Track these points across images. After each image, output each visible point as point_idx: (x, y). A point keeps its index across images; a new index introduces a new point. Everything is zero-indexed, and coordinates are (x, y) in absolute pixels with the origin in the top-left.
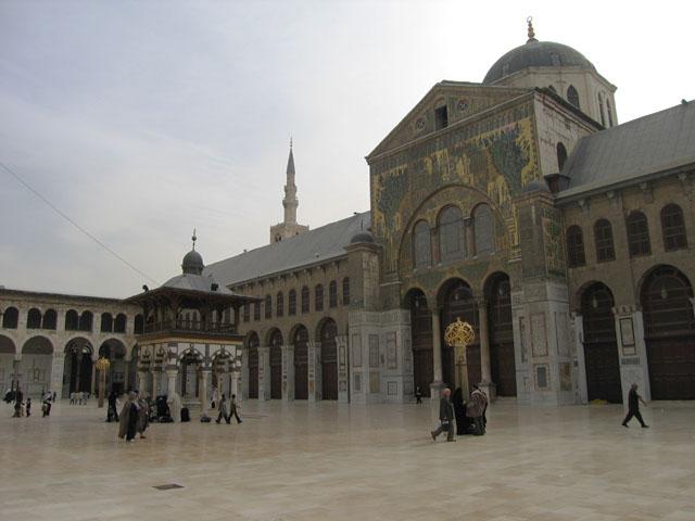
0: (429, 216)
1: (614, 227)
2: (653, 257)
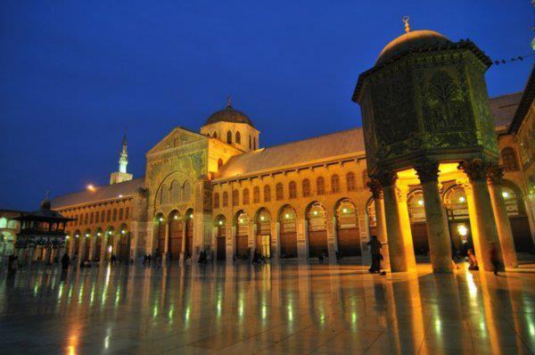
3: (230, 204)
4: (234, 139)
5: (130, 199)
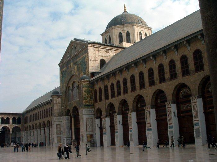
0: (70, 85)
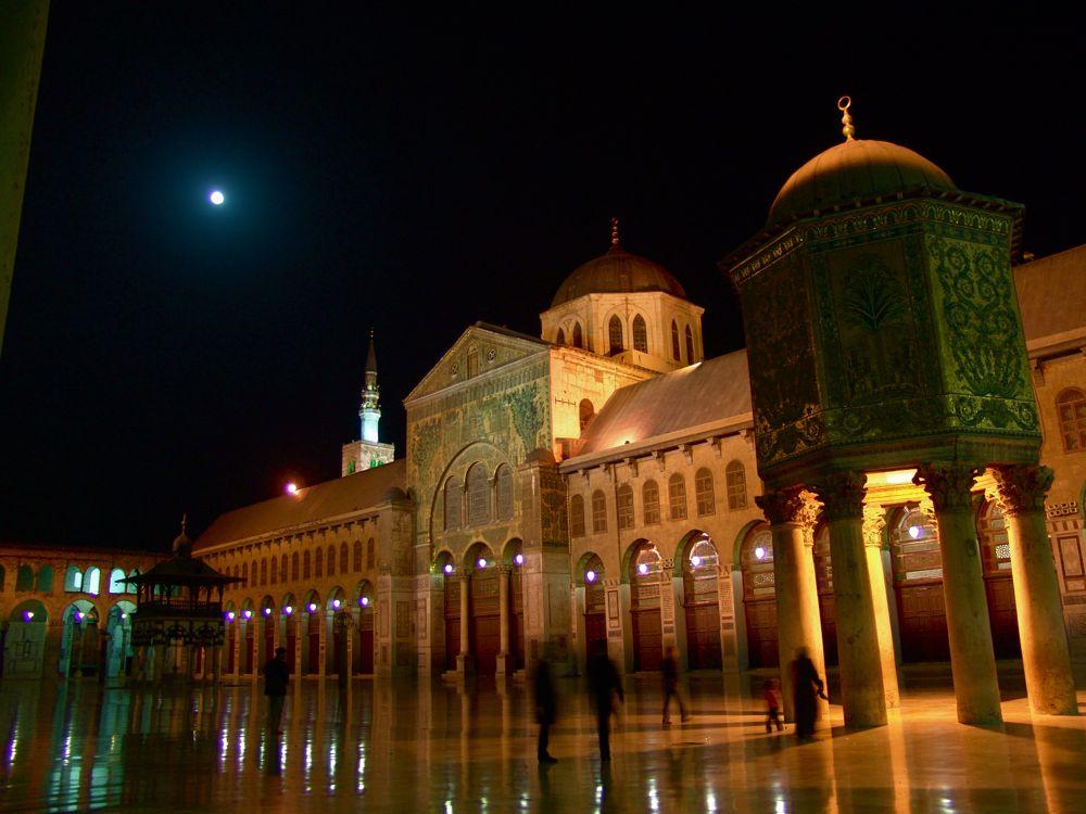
1: (608, 497)
2: (635, 531)
3: (612, 522)
4: (628, 340)
5: (375, 517)
